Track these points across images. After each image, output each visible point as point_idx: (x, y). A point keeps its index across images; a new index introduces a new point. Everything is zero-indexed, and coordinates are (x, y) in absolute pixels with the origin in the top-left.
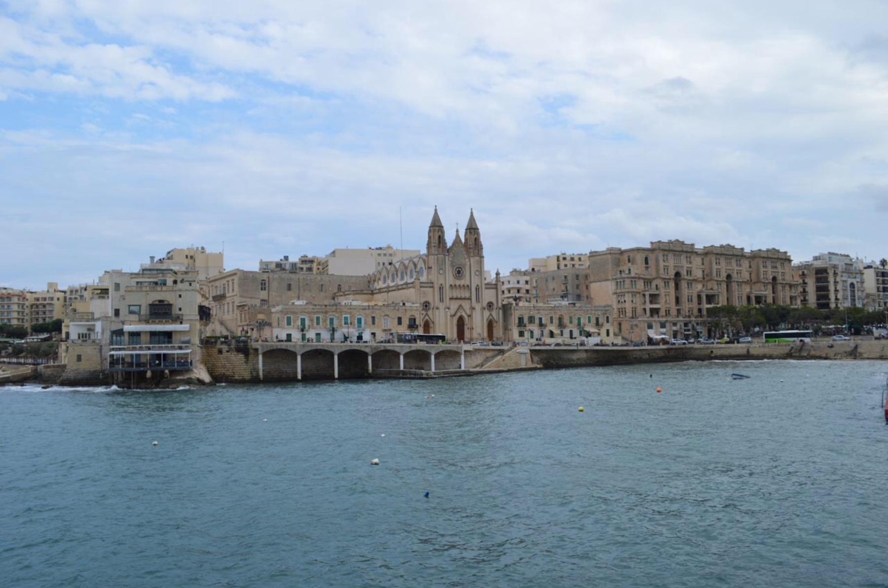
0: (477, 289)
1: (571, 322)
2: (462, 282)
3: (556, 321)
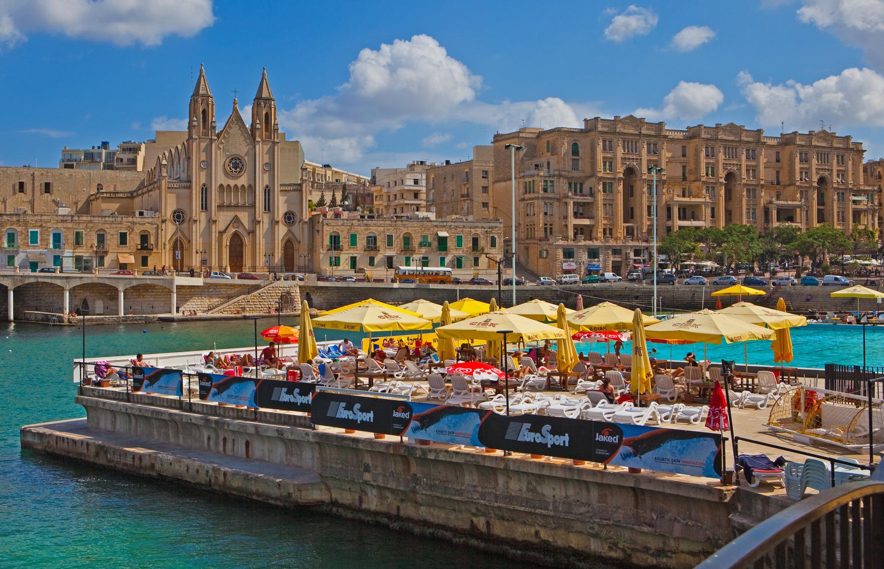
0: (268, 191)
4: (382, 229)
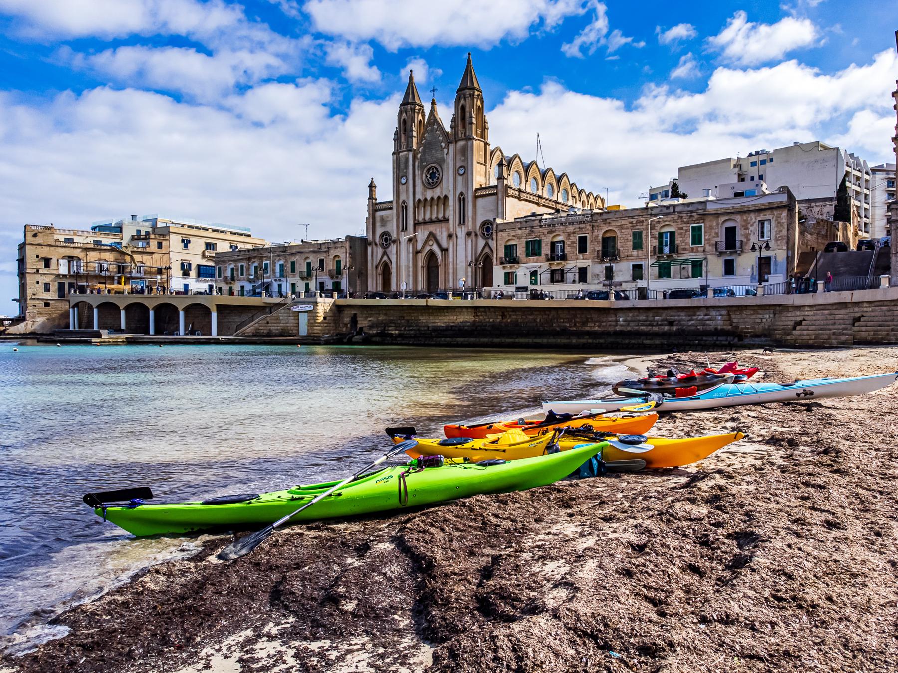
0: (462, 200)
1: (637, 245)
2: (437, 193)
3: (595, 247)
4: (571, 229)
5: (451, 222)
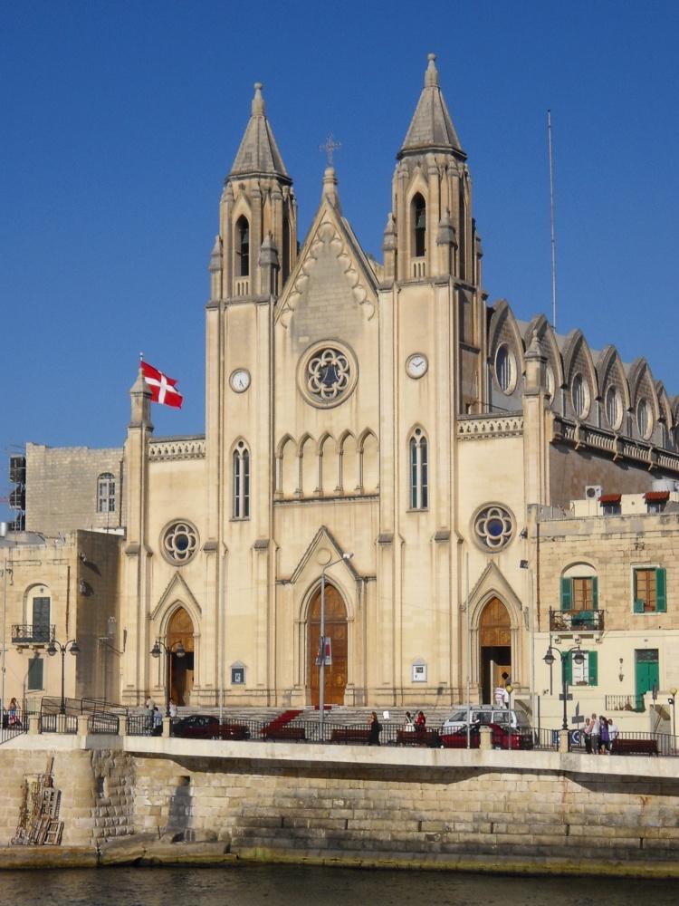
2: (340, 419)
5: (386, 500)
